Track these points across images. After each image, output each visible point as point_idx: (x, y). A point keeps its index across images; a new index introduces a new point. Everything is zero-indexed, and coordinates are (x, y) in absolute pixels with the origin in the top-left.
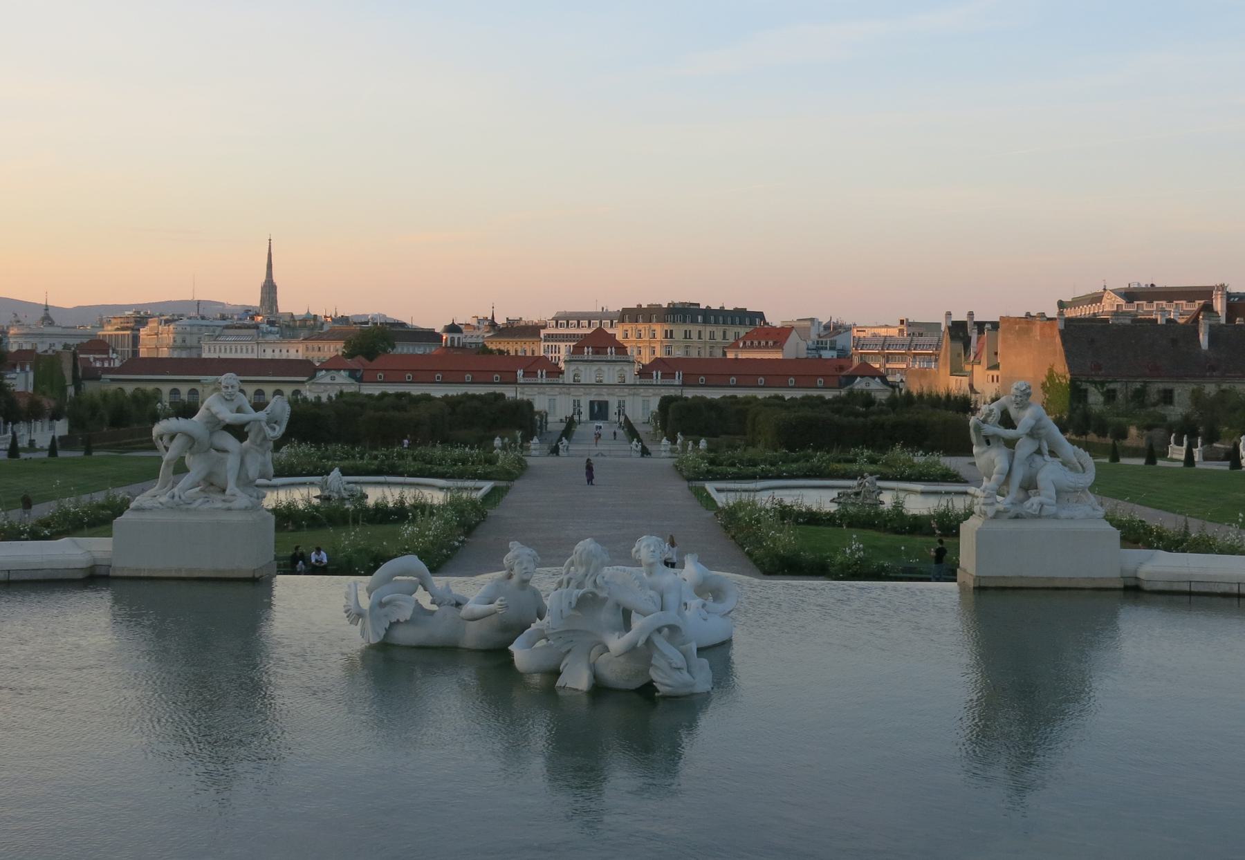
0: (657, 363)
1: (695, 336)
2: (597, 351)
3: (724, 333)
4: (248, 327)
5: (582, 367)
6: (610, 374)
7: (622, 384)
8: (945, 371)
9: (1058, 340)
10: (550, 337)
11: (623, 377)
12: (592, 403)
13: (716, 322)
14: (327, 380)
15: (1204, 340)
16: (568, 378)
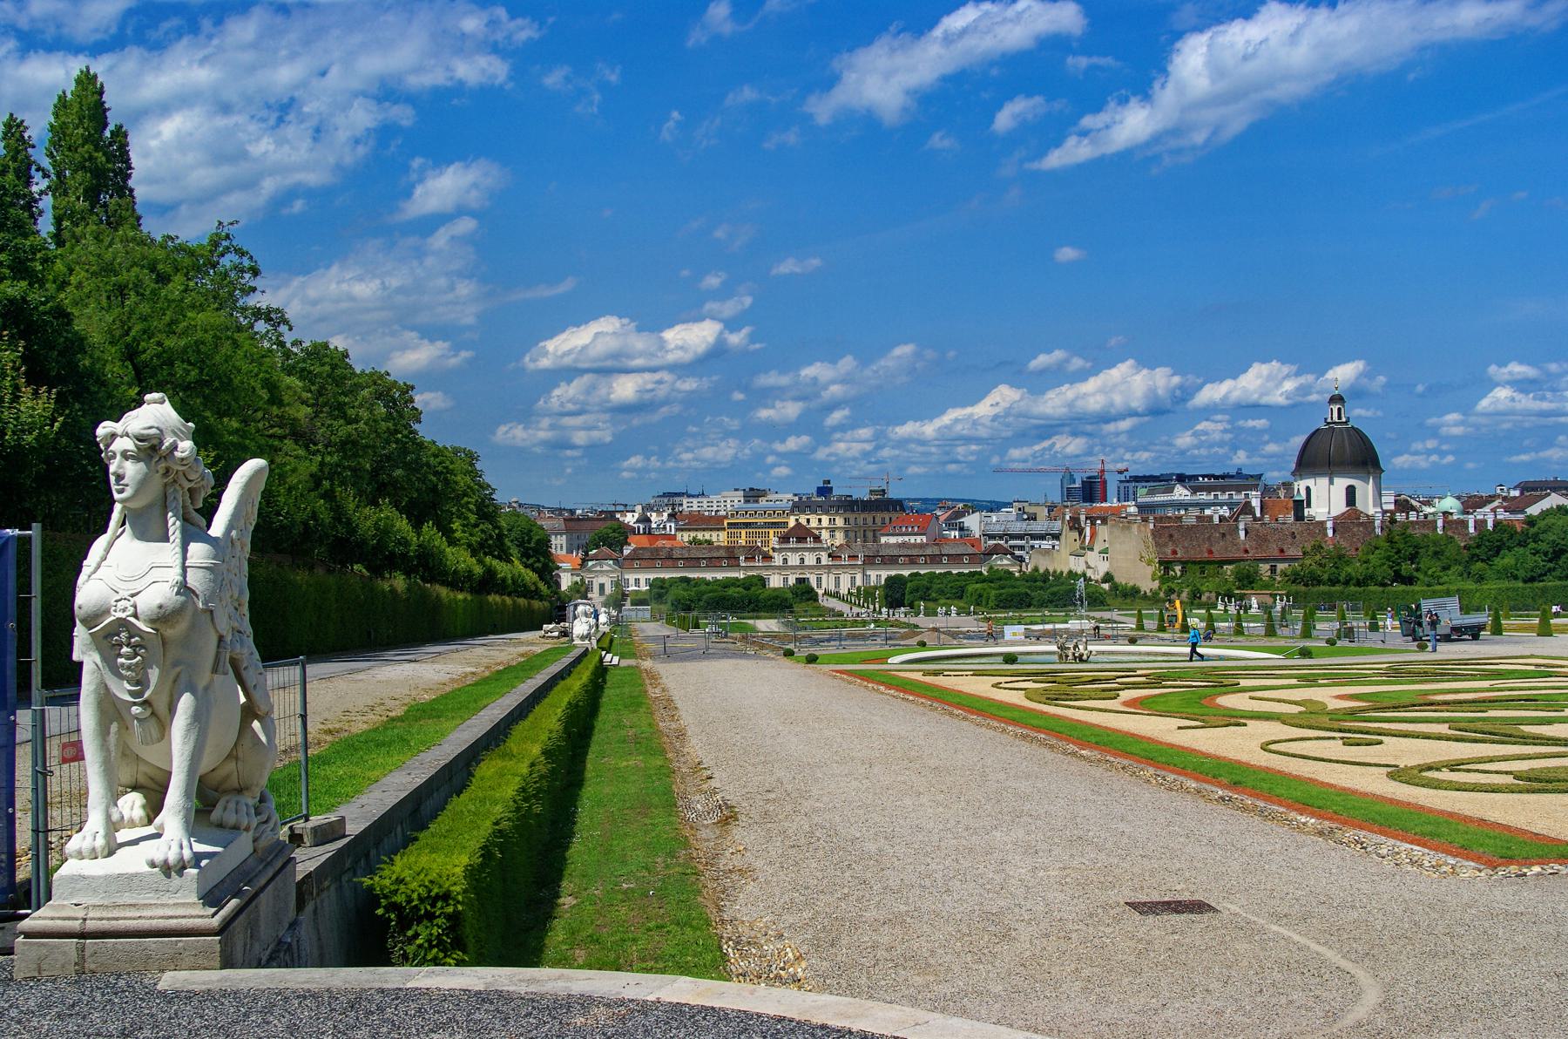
6: (810, 559)
8: (1065, 552)
11: (819, 560)
15: (1242, 534)
16: (778, 560)
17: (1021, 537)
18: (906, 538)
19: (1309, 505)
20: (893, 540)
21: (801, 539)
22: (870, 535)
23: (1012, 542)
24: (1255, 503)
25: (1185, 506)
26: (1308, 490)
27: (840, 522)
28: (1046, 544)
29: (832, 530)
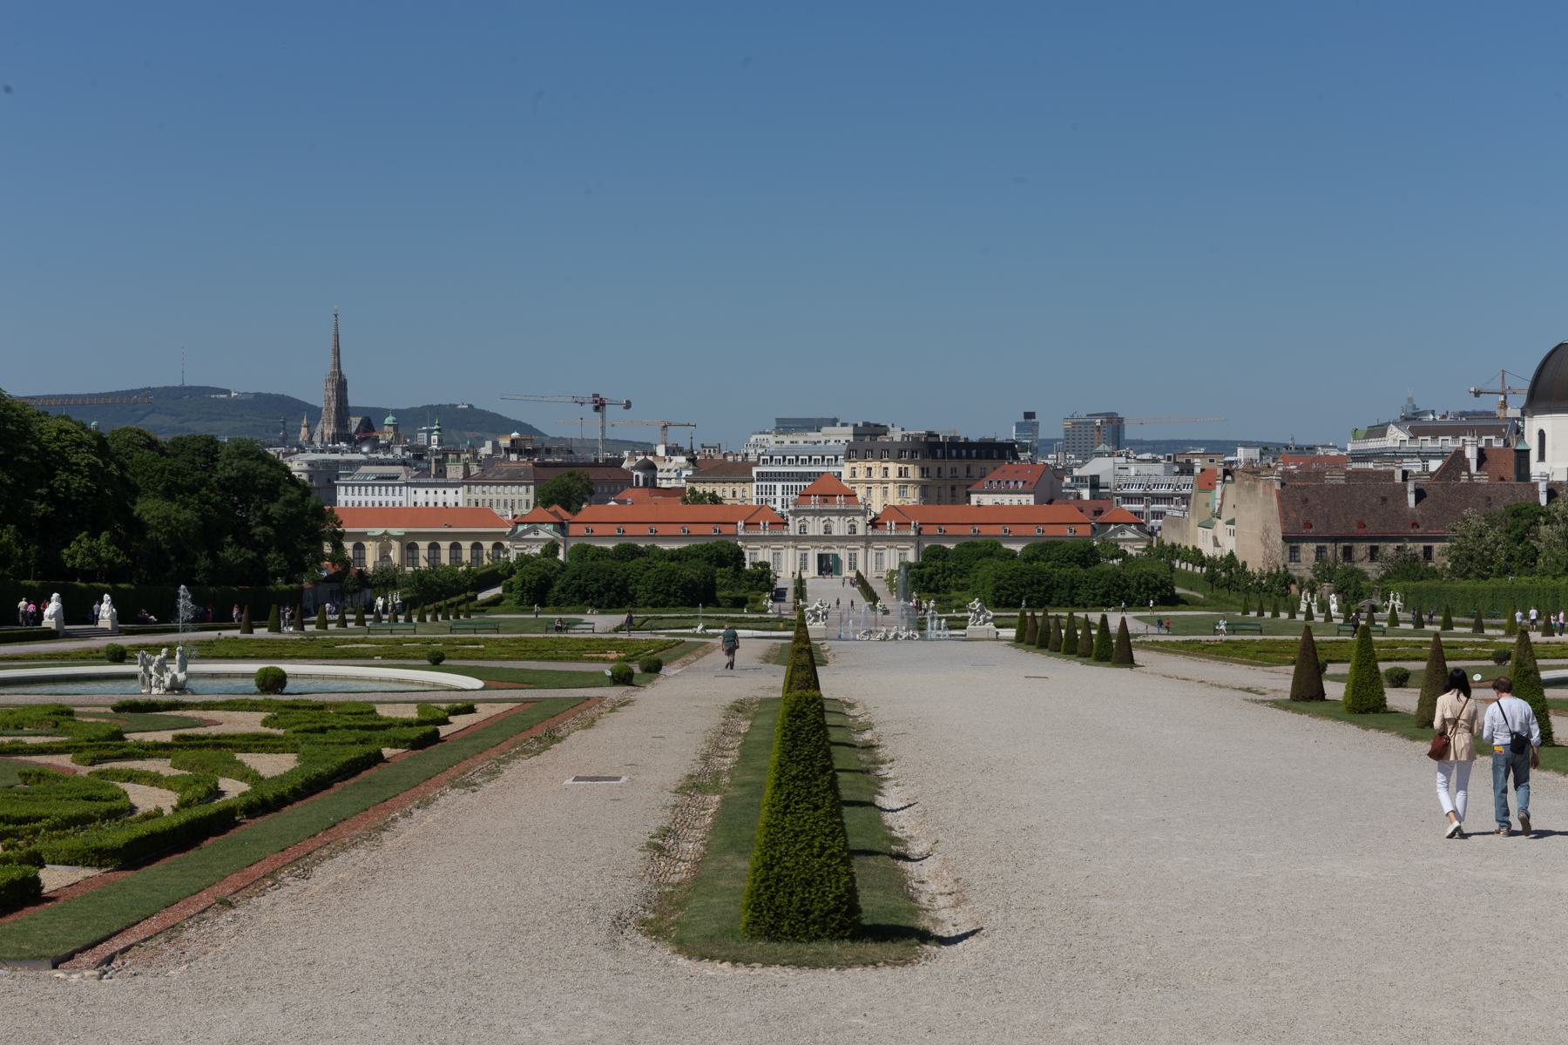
0: (889, 509)
1: (933, 472)
2: (826, 497)
3: (968, 470)
4: (393, 463)
5: (809, 519)
6: (839, 527)
7: (852, 537)
9: (1275, 499)
10: (762, 476)
11: (853, 528)
12: (820, 556)
13: (959, 457)
14: (532, 536)
15: (1411, 499)
16: (793, 528)
17: (1167, 499)
18: (999, 498)
19: (1542, 457)
20: (988, 500)
21: (826, 497)
22: (960, 493)
23: (1156, 507)
24: (1471, 453)
25: (1396, 455)
26: (1542, 434)
27: (914, 472)
28: (1173, 510)
29: (902, 488)
